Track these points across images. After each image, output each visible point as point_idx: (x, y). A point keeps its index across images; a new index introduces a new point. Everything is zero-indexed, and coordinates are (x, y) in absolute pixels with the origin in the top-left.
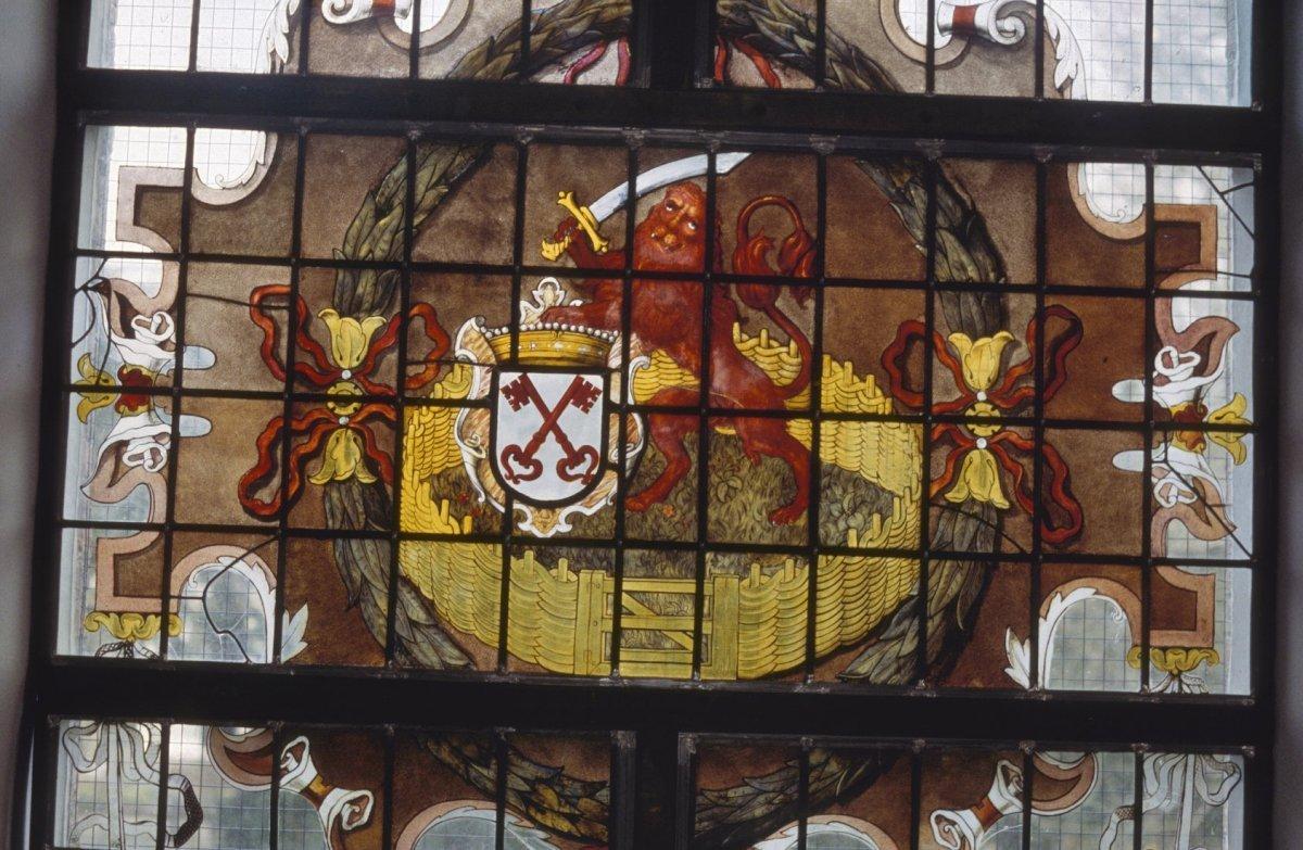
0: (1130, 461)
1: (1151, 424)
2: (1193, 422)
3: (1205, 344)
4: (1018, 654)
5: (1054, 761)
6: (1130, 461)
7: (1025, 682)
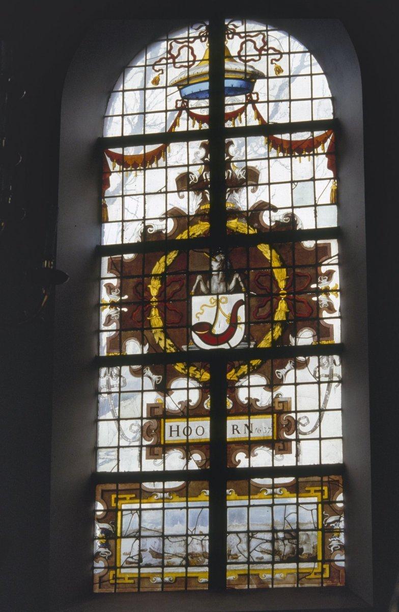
0: (315, 299)
1: (318, 292)
2: (327, 291)
3: (329, 274)
4: (292, 340)
5: (301, 358)
6: (315, 299)
7: (294, 345)
